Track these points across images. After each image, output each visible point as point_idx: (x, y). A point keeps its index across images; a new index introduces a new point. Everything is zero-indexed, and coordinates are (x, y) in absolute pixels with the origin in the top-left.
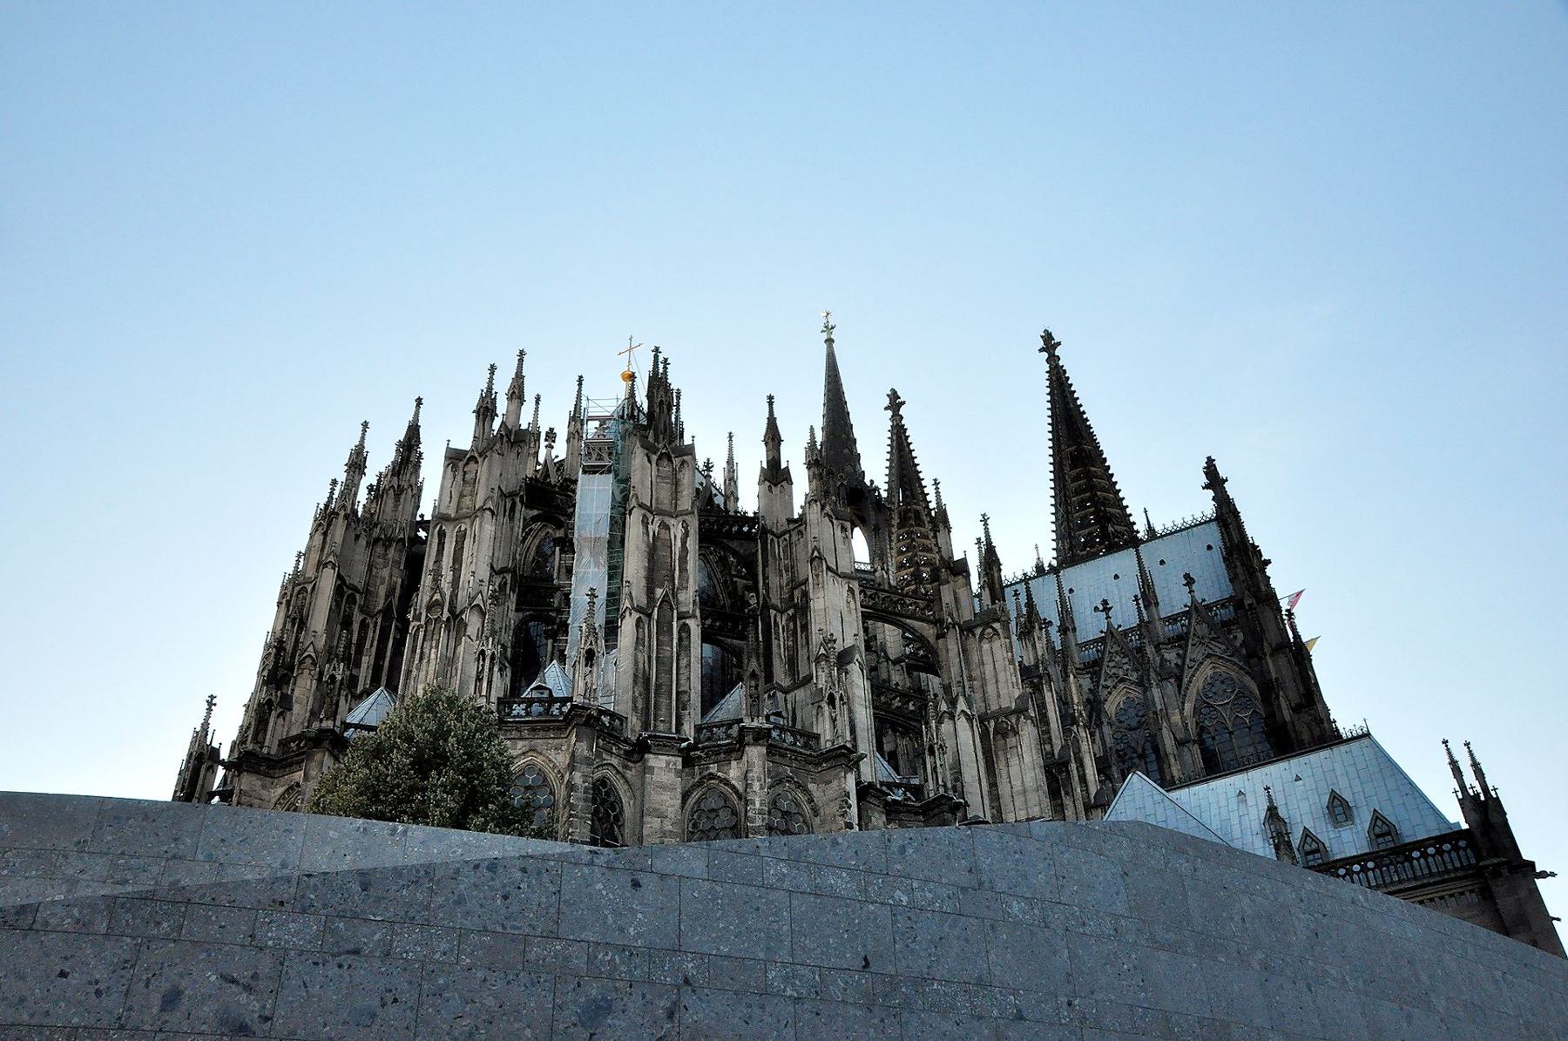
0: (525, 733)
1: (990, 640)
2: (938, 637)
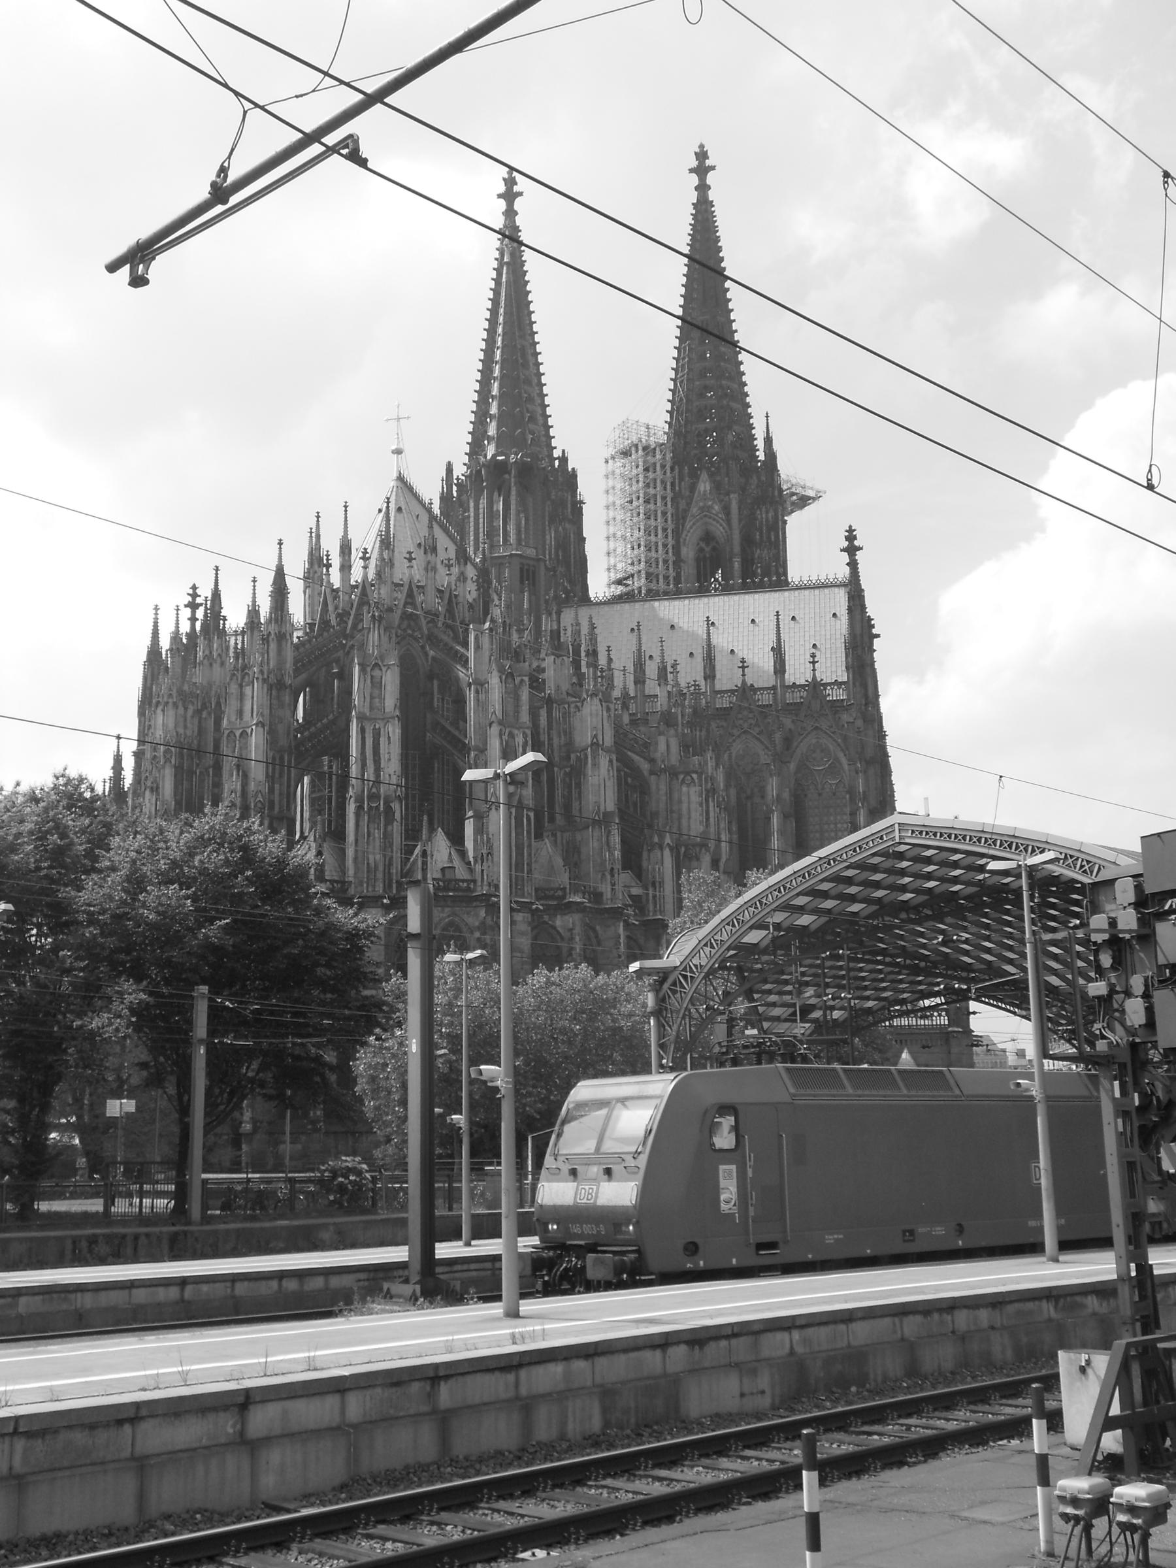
0: (449, 903)
1: (688, 785)
2: (652, 773)
